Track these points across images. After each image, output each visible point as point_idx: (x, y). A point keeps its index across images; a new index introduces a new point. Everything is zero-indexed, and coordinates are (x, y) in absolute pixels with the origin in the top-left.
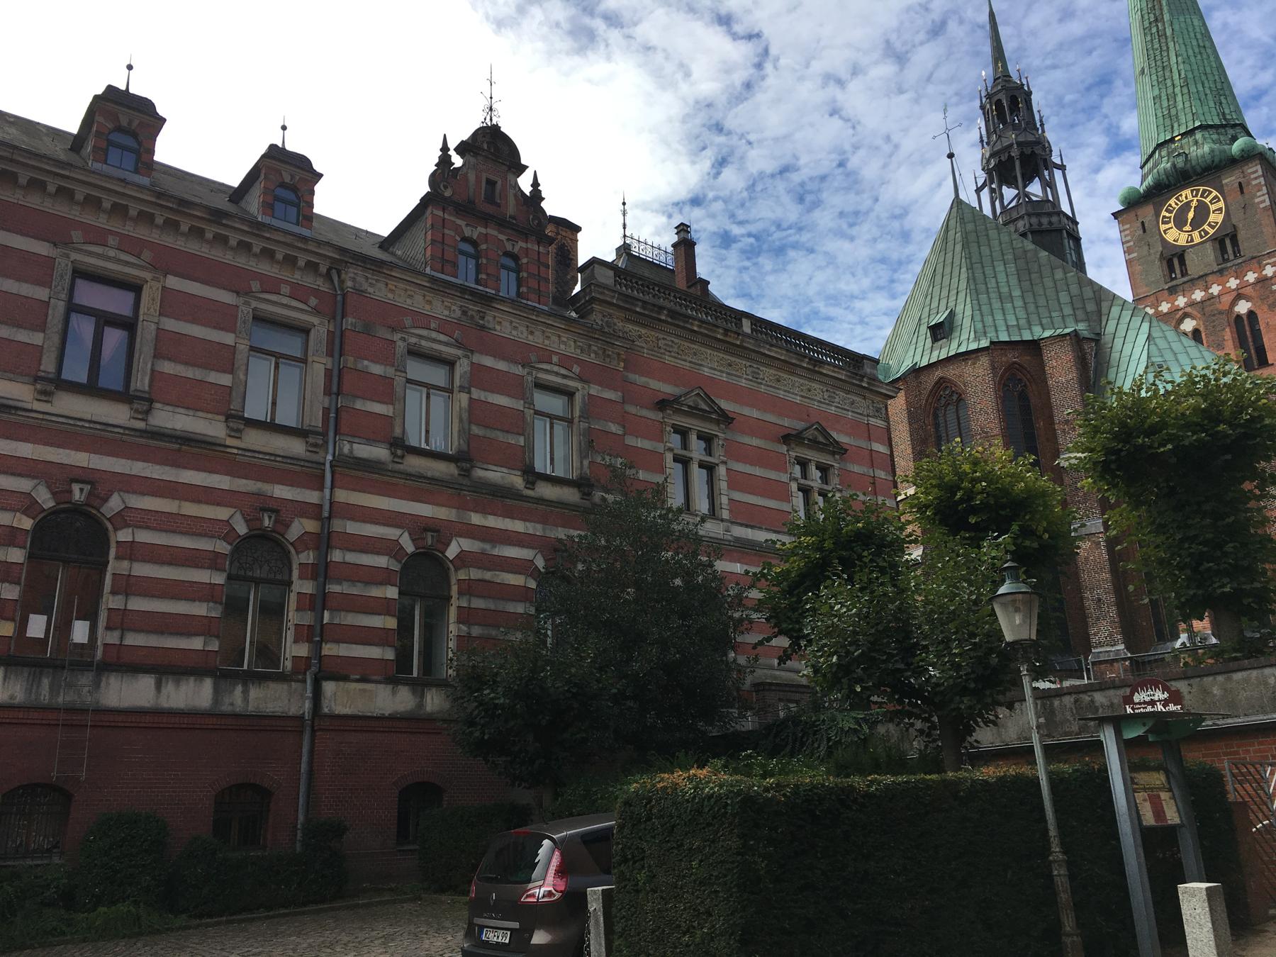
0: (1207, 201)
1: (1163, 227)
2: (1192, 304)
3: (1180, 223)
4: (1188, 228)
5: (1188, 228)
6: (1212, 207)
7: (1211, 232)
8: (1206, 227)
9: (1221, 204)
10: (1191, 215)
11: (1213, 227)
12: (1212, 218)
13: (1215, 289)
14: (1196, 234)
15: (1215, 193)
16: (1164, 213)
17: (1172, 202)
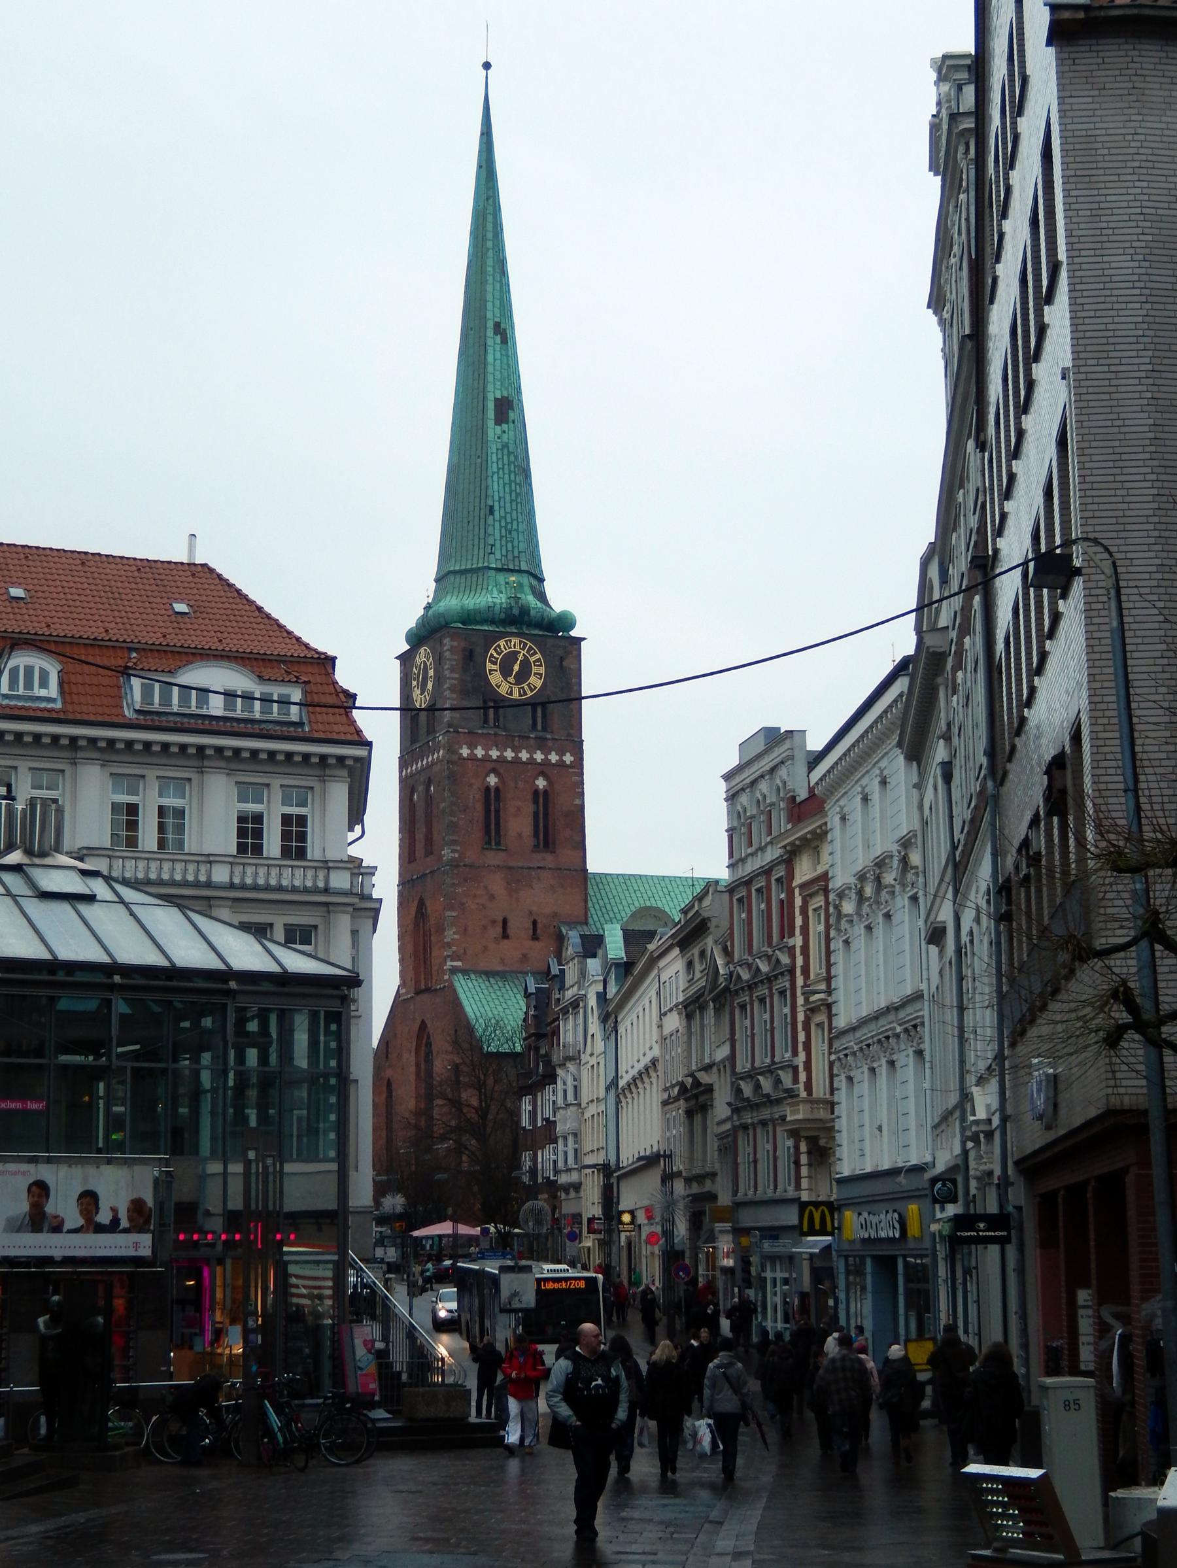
0: (532, 659)
1: (489, 666)
2: (501, 760)
3: (506, 672)
4: (511, 679)
5: (511, 679)
6: (535, 669)
7: (530, 694)
8: (525, 685)
9: (542, 670)
10: (516, 668)
11: (532, 690)
12: (533, 679)
13: (524, 755)
14: (516, 689)
15: (539, 656)
16: (492, 651)
17: (502, 643)
